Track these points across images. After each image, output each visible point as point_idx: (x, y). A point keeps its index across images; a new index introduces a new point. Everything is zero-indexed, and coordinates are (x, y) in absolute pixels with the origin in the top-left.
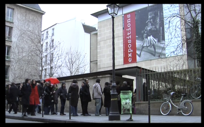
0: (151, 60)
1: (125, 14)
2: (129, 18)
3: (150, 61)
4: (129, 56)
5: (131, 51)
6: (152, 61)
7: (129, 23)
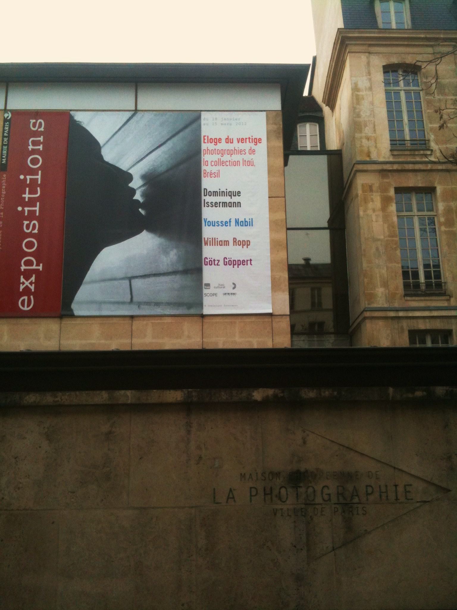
0: (132, 317)
1: (15, 113)
2: (36, 134)
3: (128, 321)
4: (22, 287)
5: (34, 267)
6: (137, 324)
7: (34, 152)
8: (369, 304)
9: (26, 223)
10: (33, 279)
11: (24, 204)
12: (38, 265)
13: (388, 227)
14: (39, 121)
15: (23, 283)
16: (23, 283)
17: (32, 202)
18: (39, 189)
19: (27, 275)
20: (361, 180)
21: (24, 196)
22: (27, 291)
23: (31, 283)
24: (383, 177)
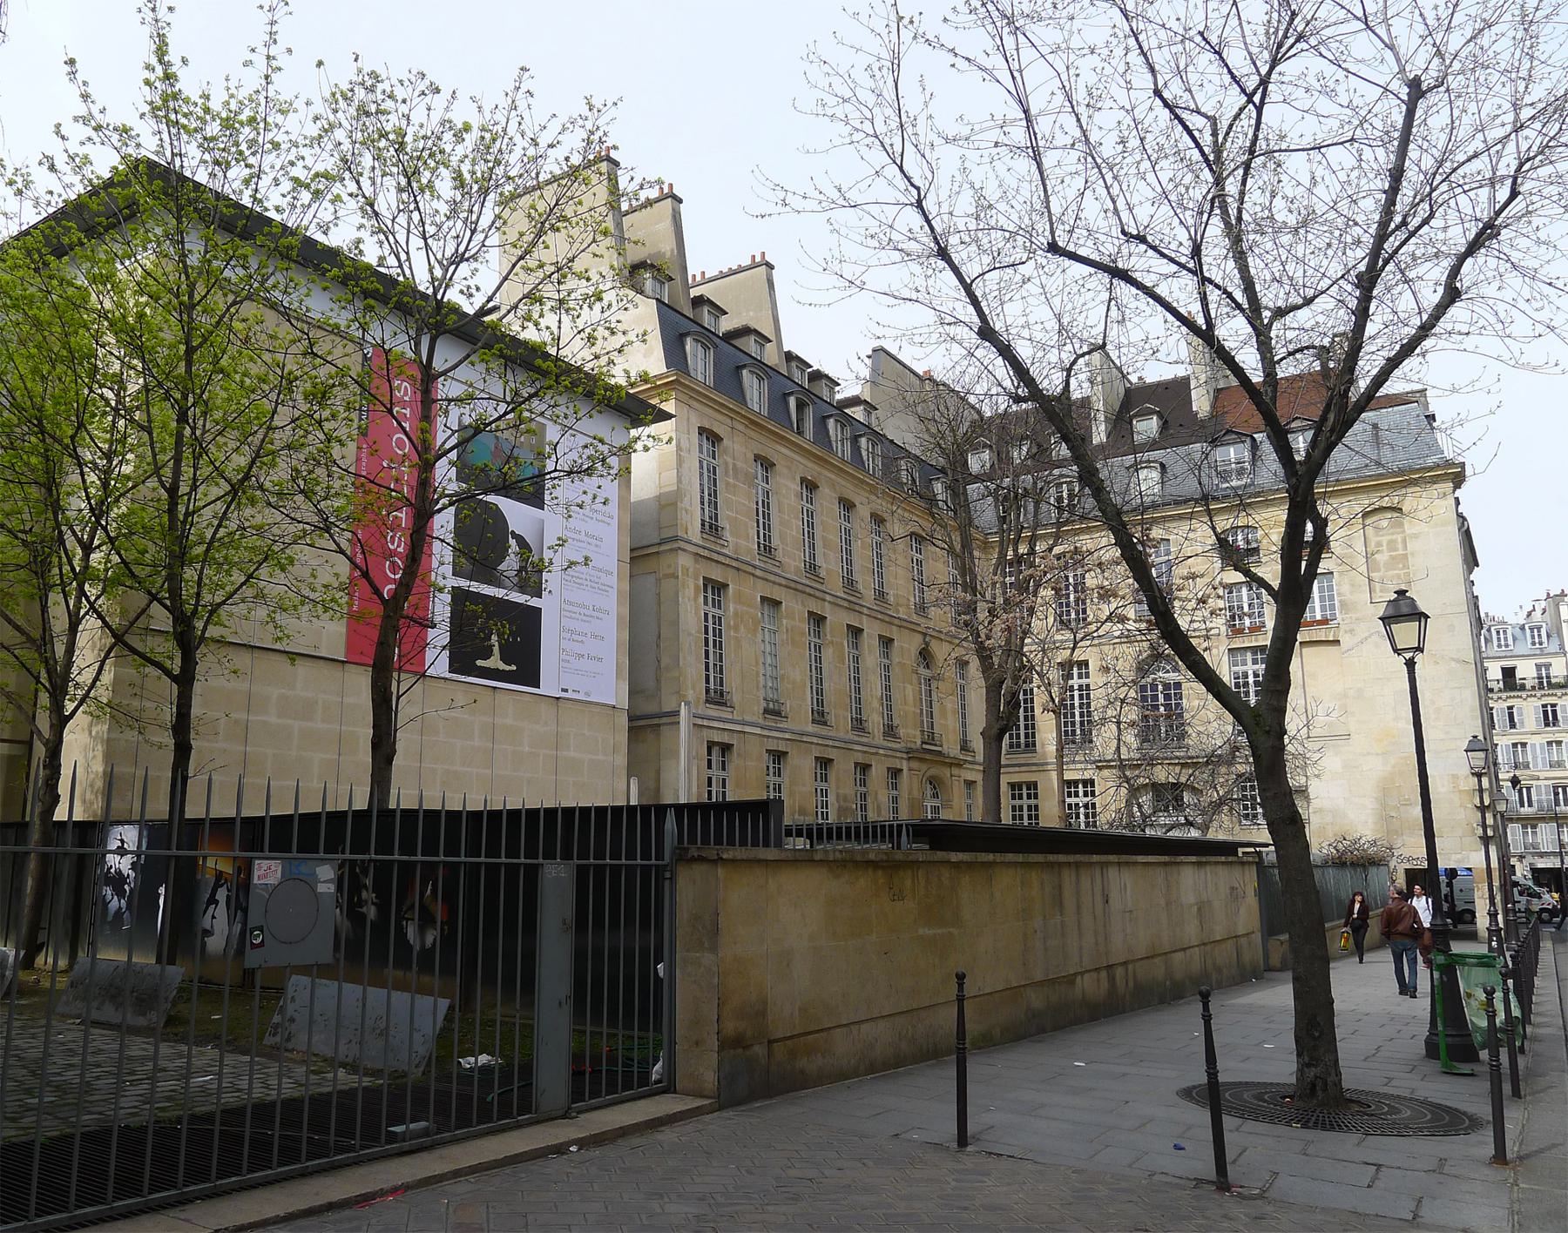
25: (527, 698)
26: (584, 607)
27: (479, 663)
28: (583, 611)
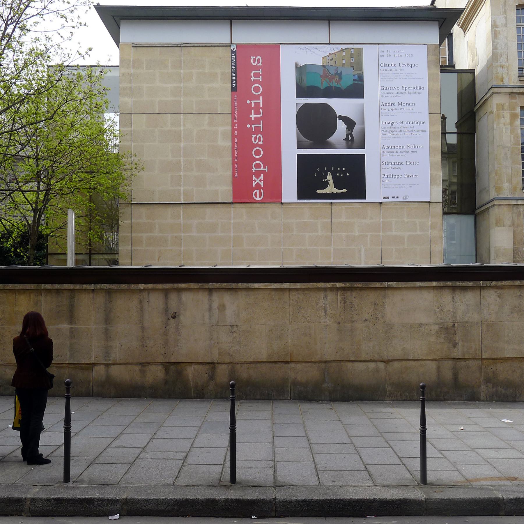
2: (257, 68)
4: (254, 184)
5: (262, 169)
7: (256, 82)
8: (497, 195)
9: (254, 136)
10: (262, 177)
11: (251, 123)
12: (264, 167)
13: (514, 138)
14: (257, 58)
15: (255, 181)
16: (255, 181)
17: (257, 121)
18: (261, 110)
19: (258, 174)
20: (495, 101)
21: (250, 116)
22: (258, 186)
23: (260, 181)
24: (512, 98)
25: (357, 205)
26: (399, 147)
27: (319, 191)
28: (398, 150)
